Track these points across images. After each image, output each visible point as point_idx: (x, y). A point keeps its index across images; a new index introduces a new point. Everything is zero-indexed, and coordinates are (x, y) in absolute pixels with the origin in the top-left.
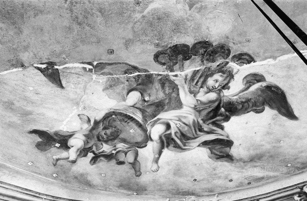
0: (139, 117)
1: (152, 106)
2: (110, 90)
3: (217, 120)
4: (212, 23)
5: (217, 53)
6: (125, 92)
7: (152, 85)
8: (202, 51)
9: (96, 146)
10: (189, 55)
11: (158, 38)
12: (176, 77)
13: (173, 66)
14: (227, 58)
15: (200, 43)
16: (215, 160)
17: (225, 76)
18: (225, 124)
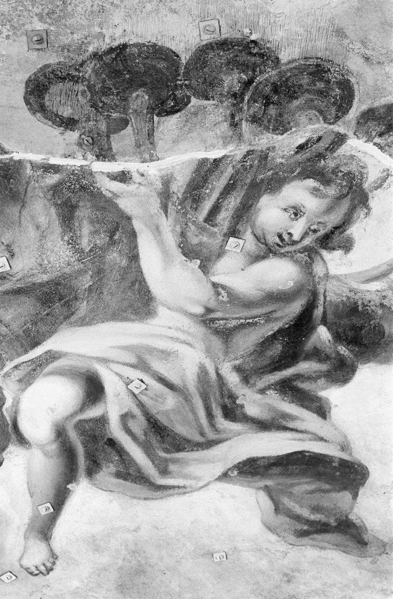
1: (23, 298)
3: (299, 377)
5: (295, 92)
7: (19, 207)
8: (232, 80)
10: (179, 93)
11: (46, 11)
13: (108, 137)
14: (337, 118)
15: (224, 44)
16: (292, 538)
17: (333, 192)
18: (333, 395)
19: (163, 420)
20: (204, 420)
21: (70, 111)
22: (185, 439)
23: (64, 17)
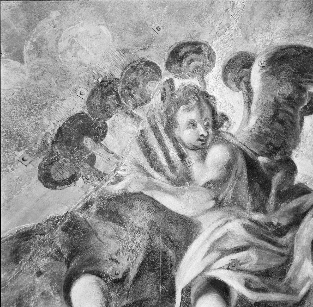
1: (144, 277)
4: (79, 53)
5: (136, 83)
7: (95, 236)
10: (99, 125)
11: (17, 146)
12: (120, 181)
13: (94, 168)
14: (160, 76)
15: (93, 93)
17: (194, 104)
19: (262, 268)
20: (275, 249)
21: (68, 173)
22: (280, 266)
23: (27, 141)
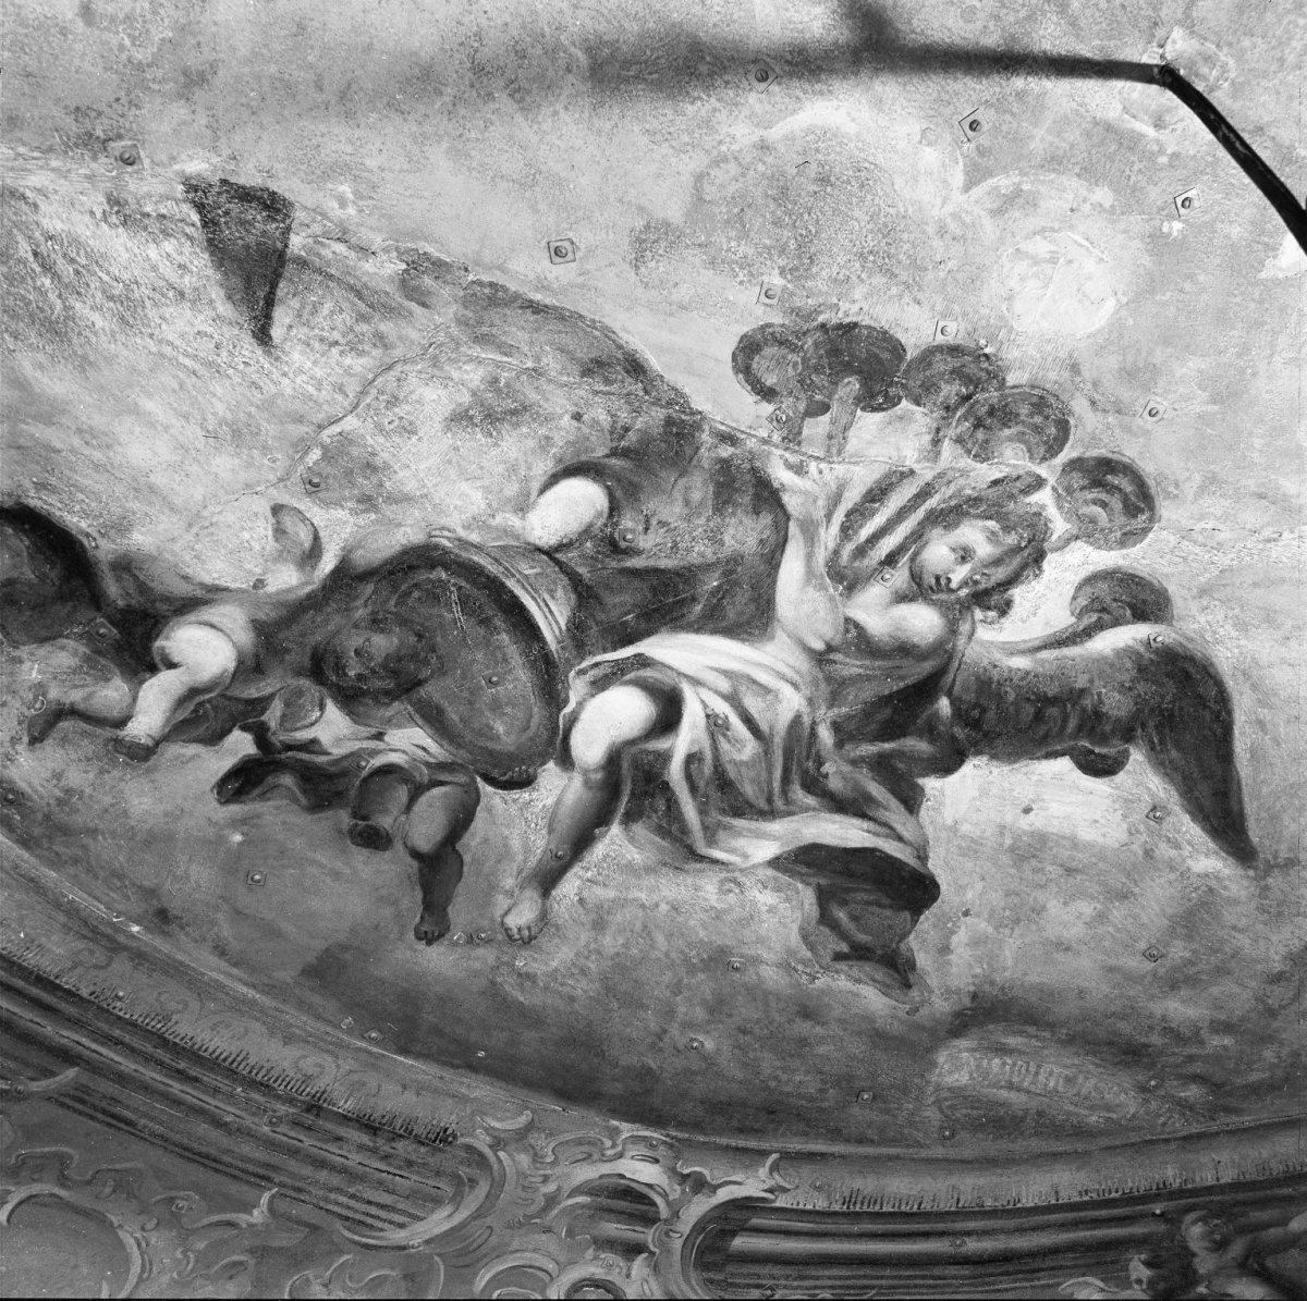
0: (552, 615)
1: (637, 583)
2: (479, 436)
3: (900, 754)
4: (1032, 283)
6: (543, 467)
8: (951, 390)
9: (287, 705)
10: (892, 391)
12: (796, 473)
13: (803, 419)
14: (1044, 459)
15: (954, 350)
17: (1010, 541)
19: (732, 773)
20: (776, 785)
21: (775, 380)
22: (747, 802)
23: (806, 278)
